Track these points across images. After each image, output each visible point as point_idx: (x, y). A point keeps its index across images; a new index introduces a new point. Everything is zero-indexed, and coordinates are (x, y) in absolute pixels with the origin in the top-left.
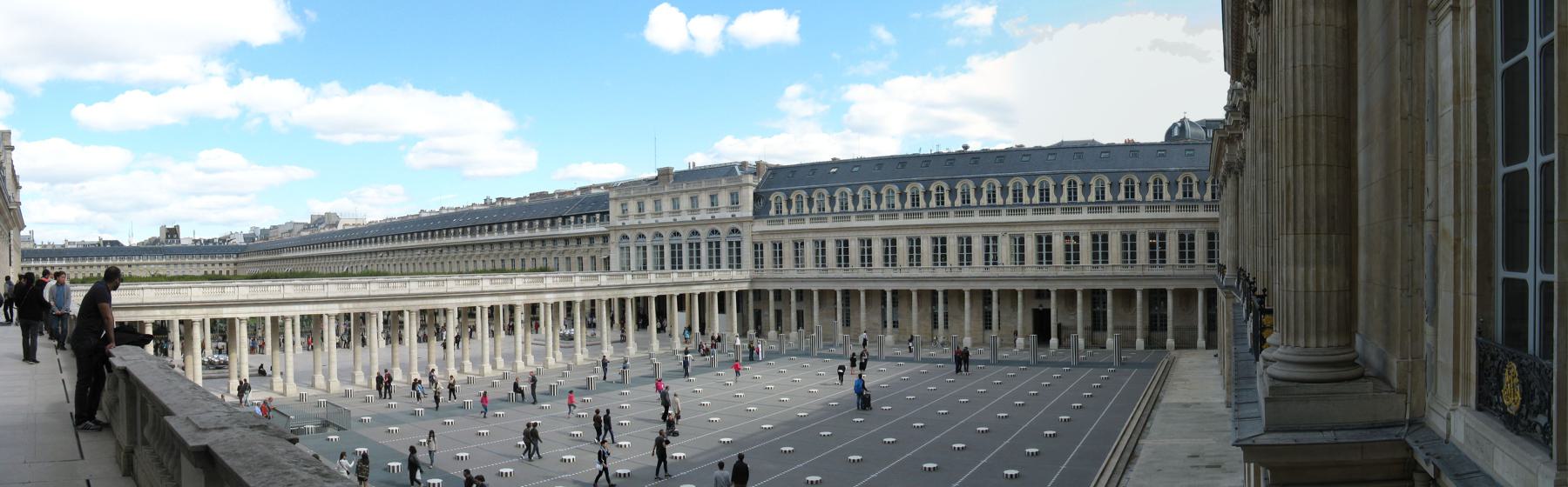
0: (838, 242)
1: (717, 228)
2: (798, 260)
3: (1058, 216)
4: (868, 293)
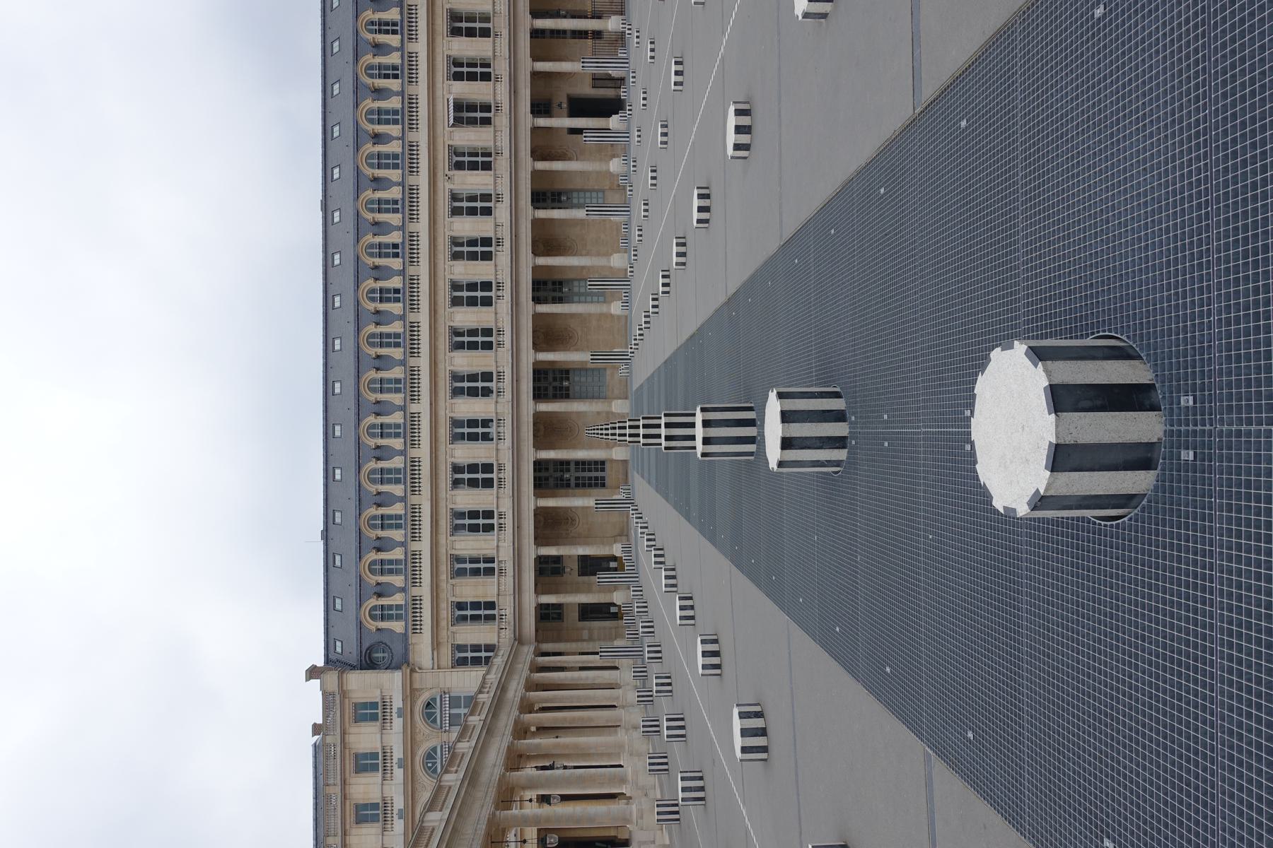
1: (421, 752)
2: (483, 567)
3: (421, 90)
4: (539, 395)
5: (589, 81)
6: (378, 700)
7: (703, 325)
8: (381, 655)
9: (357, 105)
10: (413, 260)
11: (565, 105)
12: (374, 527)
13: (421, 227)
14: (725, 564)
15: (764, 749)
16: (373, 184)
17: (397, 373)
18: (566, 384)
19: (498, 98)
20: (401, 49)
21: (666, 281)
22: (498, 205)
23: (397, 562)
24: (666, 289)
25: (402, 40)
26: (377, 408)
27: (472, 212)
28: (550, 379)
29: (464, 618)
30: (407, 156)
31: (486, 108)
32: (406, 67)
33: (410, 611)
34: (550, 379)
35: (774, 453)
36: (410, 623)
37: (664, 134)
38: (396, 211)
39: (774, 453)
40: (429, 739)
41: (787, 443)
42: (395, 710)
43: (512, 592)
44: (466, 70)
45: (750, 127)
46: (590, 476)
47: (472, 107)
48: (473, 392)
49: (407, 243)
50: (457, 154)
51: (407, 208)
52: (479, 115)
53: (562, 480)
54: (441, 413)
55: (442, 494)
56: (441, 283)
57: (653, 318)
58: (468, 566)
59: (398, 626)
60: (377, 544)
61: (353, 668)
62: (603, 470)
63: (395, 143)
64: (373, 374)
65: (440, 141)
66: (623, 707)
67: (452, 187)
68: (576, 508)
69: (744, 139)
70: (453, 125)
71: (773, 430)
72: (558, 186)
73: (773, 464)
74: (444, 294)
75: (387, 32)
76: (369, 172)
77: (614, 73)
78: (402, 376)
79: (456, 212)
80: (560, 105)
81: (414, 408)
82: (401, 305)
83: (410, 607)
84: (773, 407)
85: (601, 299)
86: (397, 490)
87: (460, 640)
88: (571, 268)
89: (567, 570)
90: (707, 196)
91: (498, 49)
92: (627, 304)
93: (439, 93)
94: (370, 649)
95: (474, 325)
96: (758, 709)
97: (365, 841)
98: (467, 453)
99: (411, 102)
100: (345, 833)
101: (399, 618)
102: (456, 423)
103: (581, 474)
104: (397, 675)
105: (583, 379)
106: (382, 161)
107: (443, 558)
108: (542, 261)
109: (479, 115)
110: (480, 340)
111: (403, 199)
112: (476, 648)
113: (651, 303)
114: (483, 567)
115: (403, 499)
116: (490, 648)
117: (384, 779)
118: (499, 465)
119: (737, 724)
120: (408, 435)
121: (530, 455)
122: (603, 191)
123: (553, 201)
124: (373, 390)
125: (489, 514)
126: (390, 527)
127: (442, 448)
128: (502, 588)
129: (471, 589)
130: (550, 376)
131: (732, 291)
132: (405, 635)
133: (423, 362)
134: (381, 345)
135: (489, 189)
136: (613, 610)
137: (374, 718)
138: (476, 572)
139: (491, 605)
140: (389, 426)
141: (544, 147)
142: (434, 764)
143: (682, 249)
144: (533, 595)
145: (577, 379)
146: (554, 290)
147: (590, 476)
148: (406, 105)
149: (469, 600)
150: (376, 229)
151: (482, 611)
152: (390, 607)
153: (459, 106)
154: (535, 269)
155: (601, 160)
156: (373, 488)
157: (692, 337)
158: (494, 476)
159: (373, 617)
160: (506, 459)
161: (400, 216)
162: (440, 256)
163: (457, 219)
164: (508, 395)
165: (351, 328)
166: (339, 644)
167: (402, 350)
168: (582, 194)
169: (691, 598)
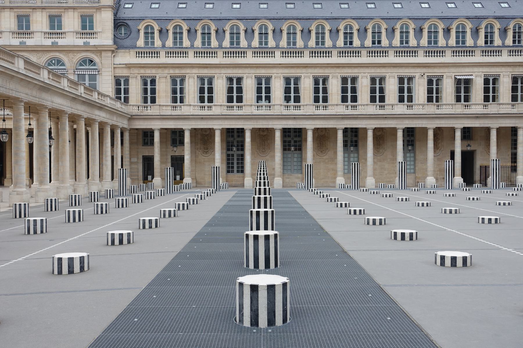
0: (230, 80)
2: (177, 96)
3: (478, 58)
4: (285, 132)
5: (485, 163)
6: (95, 30)
7: (329, 235)
8: (123, 32)
9: (468, 18)
10: (371, 53)
11: (469, 148)
12: (203, 28)
13: (391, 59)
14: (178, 249)
15: (60, 272)
16: (418, 29)
17: (300, 43)
18: (293, 148)
19: (473, 107)
20: (504, 46)
21: (358, 212)
22: (406, 107)
23: (181, 43)
24: (352, 212)
25: (509, 46)
26: (278, 30)
27: (401, 90)
28: (295, 139)
29: (145, 84)
30: (436, 49)
31: (467, 99)
32: (492, 49)
33: (150, 50)
34: (295, 139)
35: (248, 280)
36: (143, 50)
37: (451, 212)
38: (401, 42)
39: (248, 280)
40: (70, 62)
41: (254, 288)
42: (88, 40)
43: (161, 115)
44: (490, 87)
45: (455, 266)
46: (235, 164)
47: (467, 90)
48: (287, 90)
49: (382, 50)
50: (438, 81)
51: (403, 49)
52: (462, 94)
53: (232, 146)
54: (274, 71)
55: (223, 71)
56: (356, 70)
57: (334, 204)
58: (178, 87)
59: (141, 42)
60: (193, 30)
61: (115, 15)
62: (238, 172)
63: (445, 42)
64: (299, 28)
65: (446, 70)
66: (88, 183)
67: (417, 77)
68: (214, 155)
69: (448, 262)
70: (456, 78)
71: (263, 280)
72: (417, 144)
73: (241, 279)
74: (349, 73)
75: (514, 37)
76: (426, 26)
77: (490, 180)
78: (298, 46)
79: (401, 80)
80: (469, 145)
81: (278, 53)
82: (342, 45)
83: (153, 50)
84: (277, 280)
85: (346, 171)
86: (226, 43)
87: (132, 82)
88: (366, 153)
89: (175, 149)
90: (411, 238)
91: (504, 106)
92: (342, 187)
93: (476, 69)
94: (127, 26)
95: (329, 91)
96: (86, 268)
97: (9, 21)
98: (249, 87)
99: (470, 52)
100: (11, 8)
101: (146, 43)
102: (268, 80)
103: (235, 158)
104: (109, 42)
105: (295, 159)
106: (433, 34)
107: (183, 71)
108: (370, 134)
109: (462, 94)
110: (320, 94)
111: (409, 47)
112: (126, 91)
113: (344, 203)
114: (177, 96)
115: (220, 47)
116: (126, 100)
117: (45, 33)
118: (241, 107)
119: (76, 255)
120: (261, 50)
121: (248, 126)
122: (414, 173)
123: (408, 141)
124: (289, 28)
125: (210, 100)
126: (203, 38)
127: (252, 71)
128: (164, 108)
129: (163, 89)
130: (297, 139)
131: (351, 254)
132: (135, 47)
133: (306, 59)
134: (317, 33)
135: (415, 101)
136: (150, 177)
137: (84, 27)
138: (174, 91)
139: (153, 101)
140: (266, 38)
141: (442, 135)
142: (54, 64)
143: (378, 223)
144: (160, 127)
145: (296, 155)
146: (351, 142)
147: (235, 164)
148: (468, 49)
149: (157, 87)
150: (390, 30)
151: (150, 95)
152: (153, 38)
153: (468, 82)
154: (365, 130)
155: (434, 171)
156: (227, 28)
157: (322, 229)
158: (235, 103)
159: (147, 27)
160: (246, 111)
161: (399, 45)
162: (373, 70)
163: (396, 81)
164: (285, 112)
165: (328, 15)
166: (130, 6)
167: (314, 46)
168: (412, 159)
169: (156, 226)
